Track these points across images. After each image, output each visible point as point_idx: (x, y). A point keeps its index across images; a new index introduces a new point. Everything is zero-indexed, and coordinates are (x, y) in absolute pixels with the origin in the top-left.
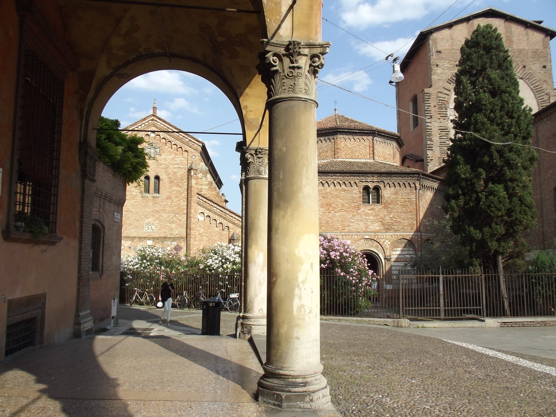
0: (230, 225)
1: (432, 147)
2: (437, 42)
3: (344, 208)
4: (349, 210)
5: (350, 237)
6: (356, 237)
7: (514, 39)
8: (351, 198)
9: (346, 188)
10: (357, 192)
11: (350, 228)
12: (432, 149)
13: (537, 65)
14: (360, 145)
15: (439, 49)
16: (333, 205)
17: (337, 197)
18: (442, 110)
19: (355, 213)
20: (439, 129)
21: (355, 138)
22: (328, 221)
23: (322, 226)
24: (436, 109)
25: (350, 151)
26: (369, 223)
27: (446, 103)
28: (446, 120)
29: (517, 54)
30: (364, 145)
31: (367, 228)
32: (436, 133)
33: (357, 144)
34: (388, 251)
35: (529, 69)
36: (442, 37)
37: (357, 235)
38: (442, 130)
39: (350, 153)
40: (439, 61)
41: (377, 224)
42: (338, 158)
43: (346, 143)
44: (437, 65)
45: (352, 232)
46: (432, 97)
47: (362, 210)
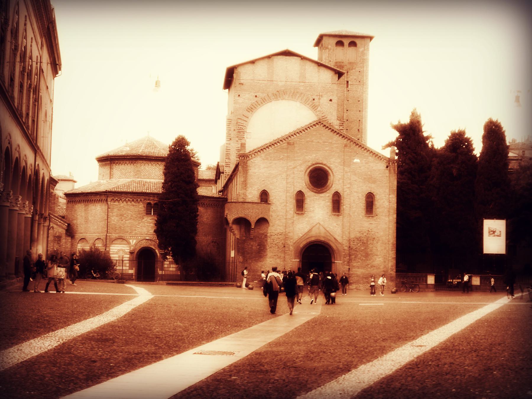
0: (55, 226)
4: (136, 219)
5: (136, 237)
6: (140, 238)
9: (134, 204)
10: (141, 207)
11: (136, 232)
14: (156, 169)
15: (242, 81)
17: (128, 210)
18: (240, 134)
19: (140, 222)
22: (121, 226)
23: (117, 229)
24: (235, 132)
29: (308, 88)
31: (148, 232)
32: (234, 153)
39: (148, 174)
40: (241, 92)
42: (138, 178)
44: (239, 96)
47: (145, 219)
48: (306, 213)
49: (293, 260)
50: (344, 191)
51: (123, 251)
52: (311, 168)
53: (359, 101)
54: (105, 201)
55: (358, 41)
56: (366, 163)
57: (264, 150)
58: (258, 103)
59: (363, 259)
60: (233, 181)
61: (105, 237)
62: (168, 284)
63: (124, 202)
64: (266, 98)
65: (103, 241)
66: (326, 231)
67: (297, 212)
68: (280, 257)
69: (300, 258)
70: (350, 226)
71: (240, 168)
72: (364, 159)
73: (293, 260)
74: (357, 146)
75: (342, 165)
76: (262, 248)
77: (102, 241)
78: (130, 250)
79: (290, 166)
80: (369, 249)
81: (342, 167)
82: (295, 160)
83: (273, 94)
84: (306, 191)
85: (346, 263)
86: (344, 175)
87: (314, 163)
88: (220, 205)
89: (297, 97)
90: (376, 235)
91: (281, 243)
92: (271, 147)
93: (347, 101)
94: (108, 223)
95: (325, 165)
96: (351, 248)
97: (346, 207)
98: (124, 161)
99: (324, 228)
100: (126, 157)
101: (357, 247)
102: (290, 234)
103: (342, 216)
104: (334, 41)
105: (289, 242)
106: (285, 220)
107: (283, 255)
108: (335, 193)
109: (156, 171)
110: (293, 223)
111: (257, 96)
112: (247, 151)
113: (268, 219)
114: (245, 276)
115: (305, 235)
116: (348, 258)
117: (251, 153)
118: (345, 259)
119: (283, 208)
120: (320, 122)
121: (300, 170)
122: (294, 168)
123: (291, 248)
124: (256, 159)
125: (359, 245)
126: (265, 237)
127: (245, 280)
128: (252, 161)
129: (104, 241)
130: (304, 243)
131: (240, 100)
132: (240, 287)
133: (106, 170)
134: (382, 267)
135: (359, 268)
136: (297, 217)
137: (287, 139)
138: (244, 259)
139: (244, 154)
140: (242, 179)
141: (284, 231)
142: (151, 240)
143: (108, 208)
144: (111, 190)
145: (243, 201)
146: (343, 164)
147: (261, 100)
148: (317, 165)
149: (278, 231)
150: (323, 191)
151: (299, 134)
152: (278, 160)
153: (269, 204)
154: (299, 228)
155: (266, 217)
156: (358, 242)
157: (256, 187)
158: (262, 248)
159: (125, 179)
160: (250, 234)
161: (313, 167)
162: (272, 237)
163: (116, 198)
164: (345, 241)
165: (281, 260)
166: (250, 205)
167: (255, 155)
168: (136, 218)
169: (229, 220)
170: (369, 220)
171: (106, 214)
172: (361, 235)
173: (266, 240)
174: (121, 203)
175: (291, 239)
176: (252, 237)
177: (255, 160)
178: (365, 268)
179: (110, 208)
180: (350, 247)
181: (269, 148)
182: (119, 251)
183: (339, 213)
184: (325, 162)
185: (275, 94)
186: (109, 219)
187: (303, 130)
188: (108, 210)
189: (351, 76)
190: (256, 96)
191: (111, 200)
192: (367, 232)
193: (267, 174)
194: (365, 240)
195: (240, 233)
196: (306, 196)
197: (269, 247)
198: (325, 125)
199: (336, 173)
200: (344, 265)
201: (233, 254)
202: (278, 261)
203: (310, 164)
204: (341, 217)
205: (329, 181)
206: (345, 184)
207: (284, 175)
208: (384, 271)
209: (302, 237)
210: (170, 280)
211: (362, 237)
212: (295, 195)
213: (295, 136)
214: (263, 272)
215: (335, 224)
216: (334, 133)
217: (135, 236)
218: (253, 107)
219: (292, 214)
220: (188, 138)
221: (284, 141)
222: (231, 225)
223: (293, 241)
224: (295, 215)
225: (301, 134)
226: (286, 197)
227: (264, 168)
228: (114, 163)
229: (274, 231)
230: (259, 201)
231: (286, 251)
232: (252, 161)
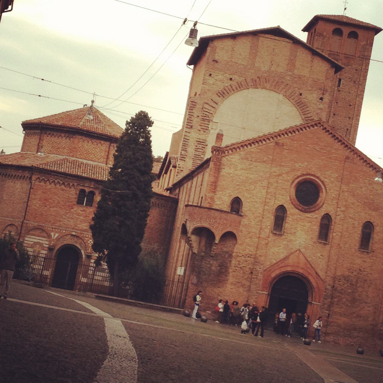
1: (185, 158)
2: (215, 50)
3: (59, 205)
4: (63, 207)
5: (59, 230)
6: (64, 231)
7: (298, 64)
8: (67, 197)
9: (64, 188)
10: (73, 193)
12: (184, 159)
13: (315, 95)
15: (217, 58)
16: (50, 201)
18: (205, 122)
20: (197, 141)
21: (93, 141)
24: (198, 120)
25: (86, 152)
26: (79, 222)
27: (210, 116)
28: (205, 133)
30: (100, 149)
32: (193, 144)
33: (94, 147)
34: (90, 249)
35: (304, 98)
36: (223, 47)
37: (66, 230)
38: (199, 143)
41: (85, 224)
42: (73, 156)
43: (83, 144)
44: (210, 75)
45: (62, 227)
46: (198, 106)
48: (285, 234)
49: (260, 292)
50: (338, 214)
51: (41, 245)
52: (300, 179)
53: (350, 105)
54: (28, 179)
55: (360, 32)
56: (369, 184)
57: (245, 147)
58: (232, 87)
59: (347, 305)
60: (195, 179)
61: (21, 223)
62: (97, 298)
63: (52, 184)
64: (243, 83)
65: (17, 228)
66: (306, 261)
67: (275, 232)
68: (244, 285)
69: (269, 291)
70: (337, 261)
71: (211, 164)
72: (368, 179)
73: (260, 292)
74: (362, 161)
75: (339, 181)
76: (224, 271)
77: (15, 228)
78: (49, 245)
79: (274, 172)
80: (357, 292)
81: (339, 184)
82: (281, 166)
83: (252, 79)
84: (289, 207)
85: (326, 306)
86: (339, 194)
87: (304, 173)
88: (168, 206)
89: (281, 88)
90: (368, 276)
91: (248, 267)
92: (255, 145)
93: (336, 104)
94: (27, 207)
95: (318, 177)
96: (335, 288)
97: (337, 235)
98: (59, 133)
99: (305, 257)
100: (61, 129)
101: (343, 288)
102: (262, 259)
103: (329, 246)
104: (331, 27)
105: (258, 268)
106: (257, 240)
107: (248, 284)
108: (325, 216)
109: (96, 151)
110: (267, 244)
111: (233, 78)
112: (223, 145)
113: (237, 235)
114: (197, 303)
115: (280, 263)
116: (330, 300)
117: (228, 148)
118: (325, 300)
119: (256, 223)
120: (320, 123)
121: (285, 179)
122: (279, 175)
123: (260, 276)
124: (234, 157)
125: (346, 285)
126: (229, 257)
127: (197, 307)
128: (228, 158)
129: (19, 228)
130: (277, 272)
131: (211, 81)
132: (189, 315)
133: (34, 140)
134: (370, 319)
135: (341, 316)
136: (275, 238)
137: (275, 138)
138: (198, 281)
139: (220, 148)
140: (212, 179)
141: (255, 252)
142: (77, 237)
143: (31, 188)
144: (38, 166)
145: (208, 207)
146: (340, 180)
147: (237, 84)
148: (308, 177)
149: (247, 252)
150: (311, 210)
151: (291, 134)
152: (261, 162)
153: (241, 216)
154: (273, 252)
155: (235, 232)
156: (345, 281)
157: (228, 192)
158: (224, 271)
159: (55, 155)
160: (211, 251)
161: (303, 178)
162: (238, 259)
163: (43, 178)
164: (328, 278)
165: (246, 289)
166: (217, 214)
167: (232, 151)
168: (64, 206)
169: (188, 228)
170: (363, 256)
171: (26, 195)
172: (350, 274)
173: (230, 261)
174: (49, 184)
175: (261, 265)
176: (213, 254)
177: (232, 158)
178: (349, 317)
179: (33, 189)
180: (334, 287)
181: (251, 146)
182: (35, 245)
183: (327, 241)
184: (318, 174)
185: (255, 80)
186: (29, 202)
187: (298, 130)
188: (30, 191)
189: (346, 73)
190: (231, 79)
191: (37, 179)
192: (358, 271)
193: (244, 178)
194: (354, 280)
195: (199, 246)
196: (288, 212)
197: (232, 270)
198: (325, 128)
199: (330, 190)
200: (324, 308)
201: (180, 271)
202: (241, 290)
203: (299, 174)
204: (328, 247)
205: (320, 199)
206: (339, 206)
207: (265, 183)
208: (371, 325)
209: (275, 264)
210: (101, 293)
211: (351, 277)
212: (274, 210)
213: (286, 136)
214: (220, 301)
215: (319, 255)
216: (335, 139)
217: (58, 229)
218: (225, 92)
219: (268, 233)
220: (152, 116)
221: (271, 139)
222: (189, 235)
223: (264, 267)
224: (271, 235)
225: (294, 134)
226: (264, 210)
227: (243, 170)
228: (45, 133)
229: (241, 252)
230: (229, 210)
231: (252, 279)
232: (228, 158)
